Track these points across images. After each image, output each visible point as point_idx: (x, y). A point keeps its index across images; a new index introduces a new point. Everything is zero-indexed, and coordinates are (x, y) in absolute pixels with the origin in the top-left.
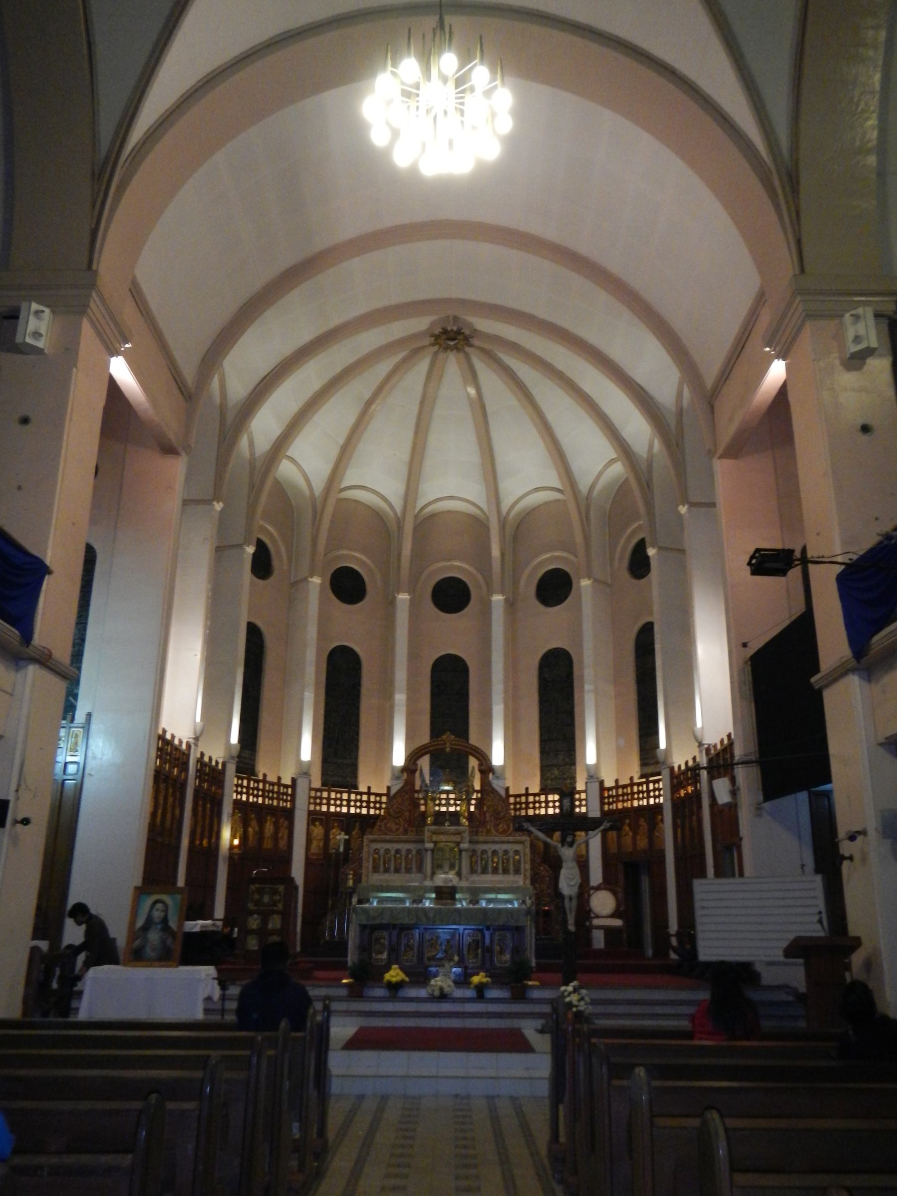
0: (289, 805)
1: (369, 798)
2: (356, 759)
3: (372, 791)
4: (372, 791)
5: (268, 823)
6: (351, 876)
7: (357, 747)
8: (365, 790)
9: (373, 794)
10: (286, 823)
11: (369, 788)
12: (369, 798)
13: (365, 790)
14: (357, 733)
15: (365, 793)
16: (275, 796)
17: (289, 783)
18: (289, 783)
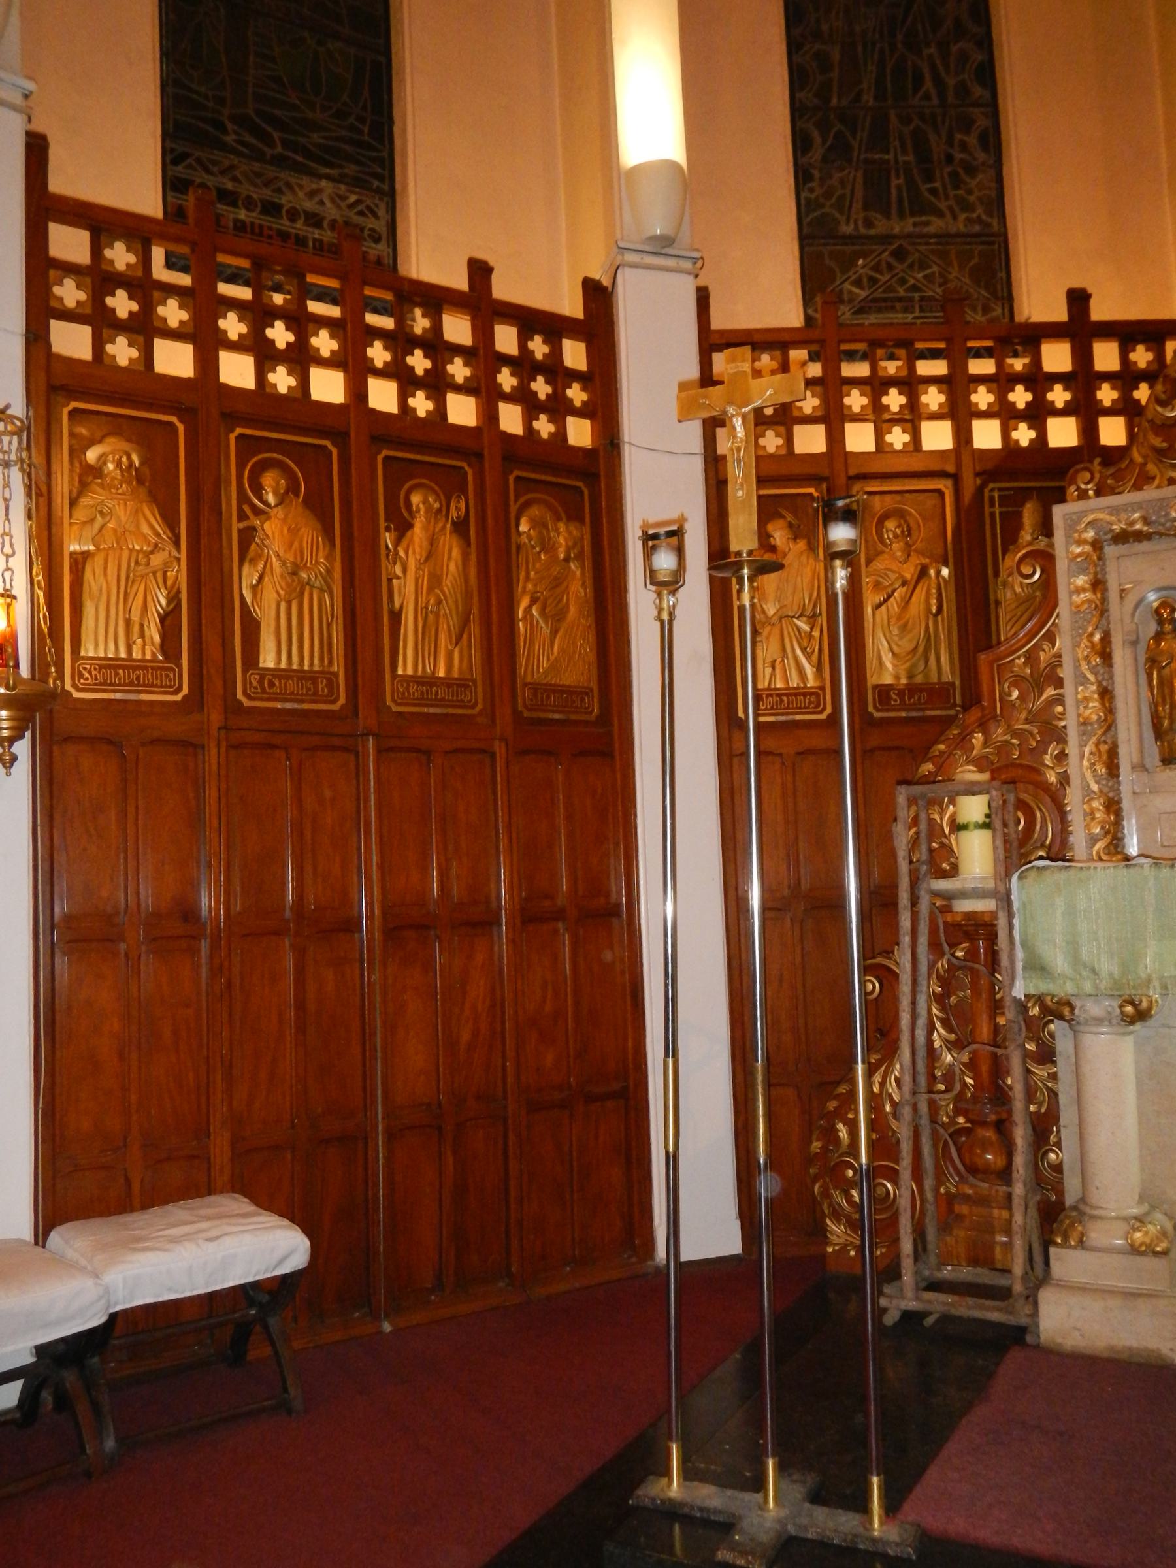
0: (579, 433)
1: (1083, 356)
2: (997, 203)
3: (1099, 312)
4: (1099, 312)
5: (418, 531)
6: (973, 808)
7: (993, 141)
8: (1059, 313)
9: (1108, 330)
10: (563, 536)
11: (1078, 299)
12: (1083, 356)
13: (1059, 313)
14: (987, 74)
15: (1053, 331)
16: (458, 370)
17: (572, 306)
18: (572, 306)
